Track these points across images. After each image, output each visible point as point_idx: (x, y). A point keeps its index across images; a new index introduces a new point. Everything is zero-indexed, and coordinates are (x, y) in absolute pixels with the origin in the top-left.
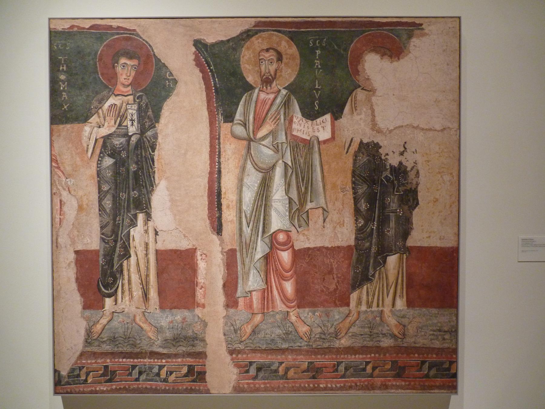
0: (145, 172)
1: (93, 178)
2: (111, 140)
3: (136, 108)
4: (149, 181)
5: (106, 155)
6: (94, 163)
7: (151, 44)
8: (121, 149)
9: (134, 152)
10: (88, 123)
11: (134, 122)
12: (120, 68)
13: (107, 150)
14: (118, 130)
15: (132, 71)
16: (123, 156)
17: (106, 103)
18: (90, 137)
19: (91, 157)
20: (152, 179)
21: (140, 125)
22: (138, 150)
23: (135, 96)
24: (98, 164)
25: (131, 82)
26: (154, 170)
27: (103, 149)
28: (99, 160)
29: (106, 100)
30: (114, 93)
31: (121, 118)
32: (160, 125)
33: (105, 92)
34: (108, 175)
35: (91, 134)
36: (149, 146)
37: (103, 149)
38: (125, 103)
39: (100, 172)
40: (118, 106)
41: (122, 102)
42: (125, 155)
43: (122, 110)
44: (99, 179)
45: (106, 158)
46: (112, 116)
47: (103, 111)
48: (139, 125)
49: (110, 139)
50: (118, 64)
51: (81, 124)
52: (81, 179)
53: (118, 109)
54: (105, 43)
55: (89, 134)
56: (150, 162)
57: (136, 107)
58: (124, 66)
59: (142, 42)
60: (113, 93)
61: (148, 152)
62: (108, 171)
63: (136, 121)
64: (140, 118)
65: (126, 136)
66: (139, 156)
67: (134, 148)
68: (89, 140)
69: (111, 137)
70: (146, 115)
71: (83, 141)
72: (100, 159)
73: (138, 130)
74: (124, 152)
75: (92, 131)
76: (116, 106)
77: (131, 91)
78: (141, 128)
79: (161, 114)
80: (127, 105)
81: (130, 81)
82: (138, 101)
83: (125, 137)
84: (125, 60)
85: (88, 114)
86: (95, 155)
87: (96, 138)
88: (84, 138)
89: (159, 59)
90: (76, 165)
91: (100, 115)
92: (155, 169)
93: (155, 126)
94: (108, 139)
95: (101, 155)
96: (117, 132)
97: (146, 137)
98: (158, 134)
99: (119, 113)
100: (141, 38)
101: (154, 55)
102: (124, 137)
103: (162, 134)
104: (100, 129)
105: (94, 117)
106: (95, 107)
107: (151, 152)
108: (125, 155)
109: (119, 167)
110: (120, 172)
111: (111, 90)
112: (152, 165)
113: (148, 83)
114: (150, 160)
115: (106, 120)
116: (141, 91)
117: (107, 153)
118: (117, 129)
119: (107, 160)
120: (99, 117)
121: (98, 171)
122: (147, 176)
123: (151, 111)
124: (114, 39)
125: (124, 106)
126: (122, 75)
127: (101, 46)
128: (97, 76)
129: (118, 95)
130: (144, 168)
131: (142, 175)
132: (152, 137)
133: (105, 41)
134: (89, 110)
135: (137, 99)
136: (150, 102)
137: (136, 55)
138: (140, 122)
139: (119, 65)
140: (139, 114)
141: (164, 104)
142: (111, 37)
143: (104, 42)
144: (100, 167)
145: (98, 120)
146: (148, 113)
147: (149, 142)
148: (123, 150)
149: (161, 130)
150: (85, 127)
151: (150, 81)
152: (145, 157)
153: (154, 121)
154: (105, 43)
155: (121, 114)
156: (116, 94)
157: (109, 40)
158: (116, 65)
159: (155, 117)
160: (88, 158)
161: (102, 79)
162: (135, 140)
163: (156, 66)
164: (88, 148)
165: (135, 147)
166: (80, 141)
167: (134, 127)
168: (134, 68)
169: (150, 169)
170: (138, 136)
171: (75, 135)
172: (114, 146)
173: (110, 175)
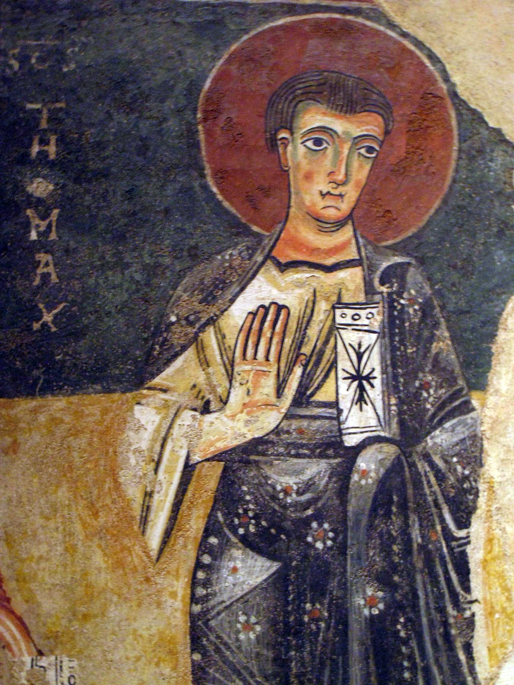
0: (424, 620)
1: (172, 653)
2: (259, 468)
3: (376, 325)
4: (446, 668)
5: (234, 539)
6: (177, 576)
7: (437, 51)
8: (310, 512)
9: (371, 527)
10: (149, 388)
11: (367, 387)
12: (301, 150)
13: (238, 516)
14: (295, 424)
15: (355, 164)
16: (319, 545)
17: (240, 299)
18: (161, 455)
19: (161, 551)
20: (462, 657)
21: (399, 398)
22: (388, 514)
23: (371, 269)
24: (194, 583)
25: (353, 209)
26: (468, 614)
27: (219, 514)
28: (199, 565)
29: (235, 288)
30: (274, 253)
31: (305, 366)
32: (491, 400)
33: (235, 252)
34: (242, 636)
35: (165, 440)
36: (441, 500)
37: (219, 514)
38: (327, 299)
39: (206, 623)
40: (295, 313)
41: (308, 296)
42: (329, 543)
43: (313, 332)
44: (197, 657)
45: (237, 553)
46: (267, 359)
47: (224, 337)
48: (393, 401)
49: (257, 462)
50: (292, 134)
51: (116, 396)
52: (110, 656)
53: (293, 325)
54: (233, 48)
55: (154, 440)
56: (446, 572)
57: (379, 318)
58: (318, 142)
59: (396, 42)
60: (268, 257)
61: (439, 528)
62: (242, 618)
63: (377, 383)
64: (394, 366)
65: (330, 452)
66: (395, 548)
67: (368, 506)
68: (156, 470)
69: (258, 454)
70: (425, 357)
71: (124, 476)
72: (206, 559)
73: (388, 423)
74: (320, 525)
75: (170, 427)
76: (283, 313)
77: (354, 248)
78: (400, 413)
79: (494, 349)
80: (334, 308)
81: (345, 206)
82: (384, 289)
83: (328, 457)
84: (324, 114)
85: (152, 349)
86: (181, 541)
87: (188, 458)
88: (133, 461)
89: (474, 112)
90: (88, 586)
91: (208, 352)
92: (476, 608)
93: (467, 403)
94: (248, 463)
95: (213, 540)
96: (288, 432)
97: (427, 457)
98: (485, 443)
99: (299, 344)
100: (392, 25)
101: (454, 95)
102: (322, 456)
103: (502, 439)
104: (209, 418)
105: (179, 362)
106: (187, 319)
107: (452, 526)
108: (329, 543)
109: (300, 598)
110: (300, 623)
111: (259, 243)
112: (459, 589)
113: (432, 211)
114: (450, 567)
115: (238, 378)
116: (395, 249)
117: (241, 531)
118: (288, 416)
119: (239, 564)
120: (205, 363)
121: (193, 618)
122: (434, 642)
123: (447, 334)
124: (273, 29)
125: (320, 316)
126: (308, 177)
127: (215, 59)
128: (196, 184)
129: (295, 264)
130: (422, 602)
131: (409, 638)
132: (456, 455)
133: (236, 38)
134: (157, 333)
135: (382, 283)
136: (439, 294)
137: (375, 97)
138: (396, 387)
139: (298, 135)
140: (394, 349)
141: (505, 303)
142: (258, 24)
143: (228, 44)
144: (206, 598)
145: (201, 378)
146: (435, 347)
147: (440, 477)
148: (318, 517)
149: (496, 421)
150: (137, 408)
151: (437, 204)
152: (422, 548)
153: (461, 383)
154: (233, 48)
155: (306, 350)
156: (283, 260)
157: (253, 33)
158: (283, 134)
159: (466, 365)
160: (146, 551)
161: (220, 197)
162: (377, 471)
163: (462, 139)
164: (148, 508)
165: (375, 499)
166: (113, 474)
167: (368, 408)
168: (363, 151)
169: (451, 611)
170: (391, 450)
171: (90, 444)
172: (274, 498)
173: (252, 636)
